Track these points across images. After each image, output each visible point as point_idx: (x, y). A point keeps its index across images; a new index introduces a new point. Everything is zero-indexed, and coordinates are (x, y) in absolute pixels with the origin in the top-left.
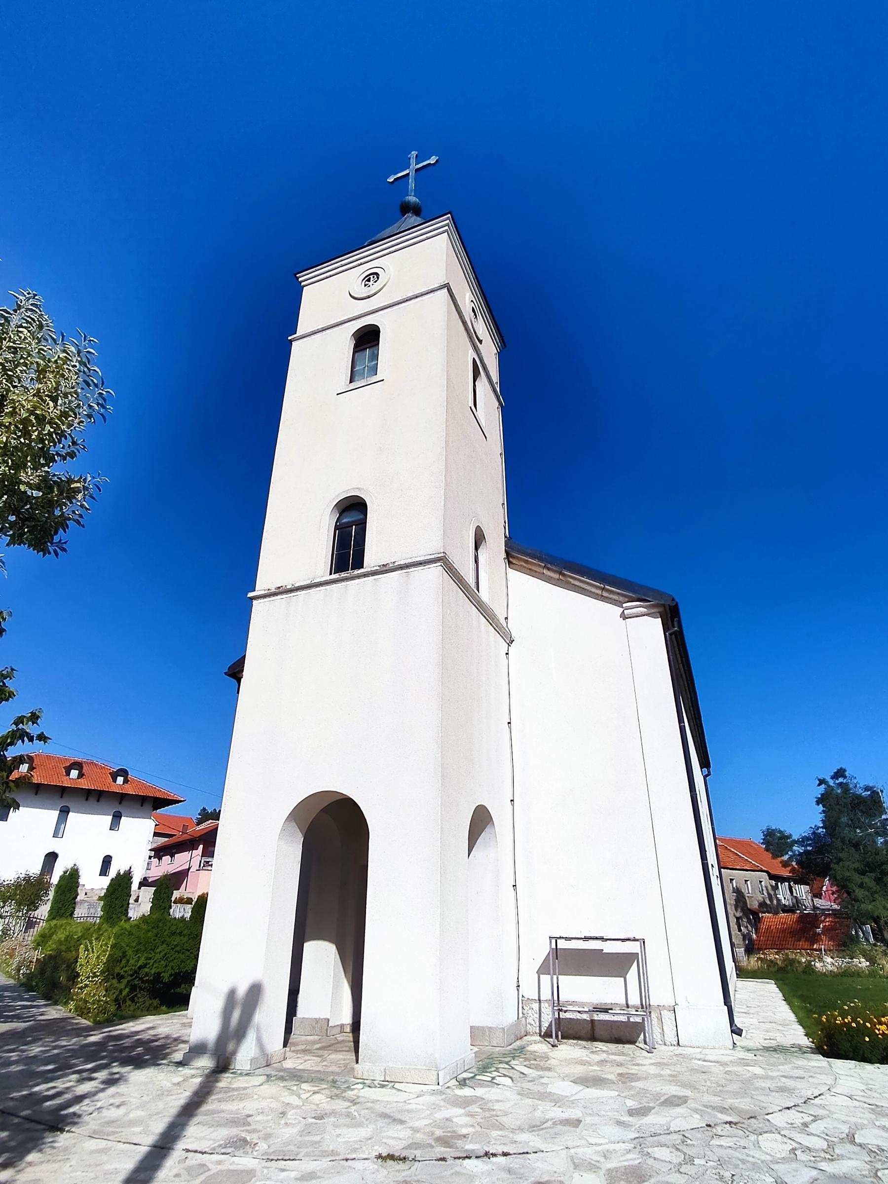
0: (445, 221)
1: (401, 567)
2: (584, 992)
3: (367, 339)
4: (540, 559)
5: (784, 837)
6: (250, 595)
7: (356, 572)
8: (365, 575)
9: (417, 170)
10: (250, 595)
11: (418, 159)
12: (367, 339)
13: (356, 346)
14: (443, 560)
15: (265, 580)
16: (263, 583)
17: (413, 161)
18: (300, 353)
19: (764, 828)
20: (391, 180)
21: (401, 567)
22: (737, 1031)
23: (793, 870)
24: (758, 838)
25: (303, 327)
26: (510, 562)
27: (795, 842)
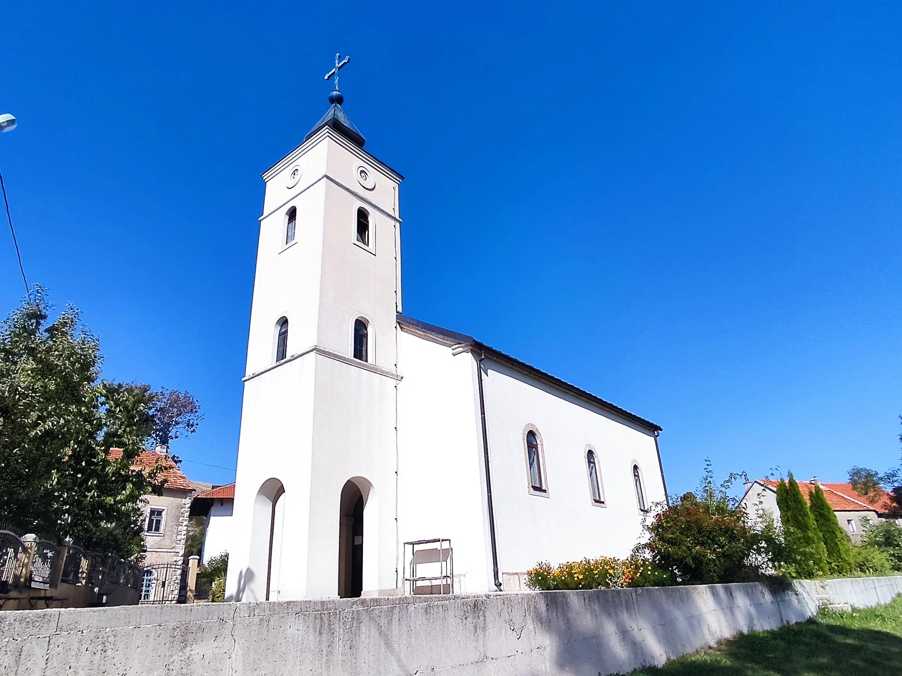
0: (326, 129)
1: (300, 356)
2: (430, 571)
3: (292, 214)
5: (869, 475)
7: (283, 361)
9: (339, 68)
11: (340, 60)
12: (292, 214)
13: (289, 219)
14: (315, 349)
15: (249, 372)
19: (850, 468)
20: (326, 77)
21: (300, 356)
22: (499, 585)
23: (885, 506)
24: (845, 479)
25: (267, 210)
26: (401, 328)
27: (881, 479)
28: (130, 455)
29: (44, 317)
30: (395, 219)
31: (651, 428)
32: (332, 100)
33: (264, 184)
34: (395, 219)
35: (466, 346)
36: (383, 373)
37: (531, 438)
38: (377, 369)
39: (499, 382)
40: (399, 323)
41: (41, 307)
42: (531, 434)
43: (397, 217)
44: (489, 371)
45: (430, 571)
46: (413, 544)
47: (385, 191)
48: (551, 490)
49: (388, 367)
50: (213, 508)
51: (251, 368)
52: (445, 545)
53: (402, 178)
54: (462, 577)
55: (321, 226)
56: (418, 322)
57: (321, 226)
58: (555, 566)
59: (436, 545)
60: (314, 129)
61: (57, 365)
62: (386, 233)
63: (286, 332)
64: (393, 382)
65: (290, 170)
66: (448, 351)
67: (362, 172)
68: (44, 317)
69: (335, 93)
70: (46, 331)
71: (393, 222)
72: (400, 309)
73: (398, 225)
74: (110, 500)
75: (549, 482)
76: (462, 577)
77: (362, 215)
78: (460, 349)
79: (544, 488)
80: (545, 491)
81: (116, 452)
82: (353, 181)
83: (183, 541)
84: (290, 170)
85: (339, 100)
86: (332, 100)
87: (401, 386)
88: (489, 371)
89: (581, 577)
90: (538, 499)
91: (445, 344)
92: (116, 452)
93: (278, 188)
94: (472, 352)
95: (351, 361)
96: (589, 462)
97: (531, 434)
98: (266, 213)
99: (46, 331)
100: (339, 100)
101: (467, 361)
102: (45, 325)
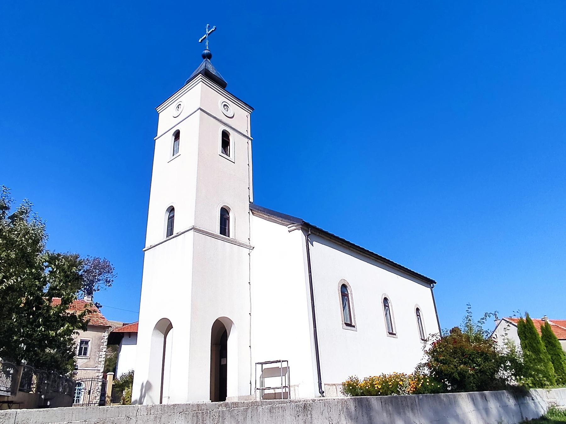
0: (200, 77)
2: (274, 382)
3: (177, 135)
4: (261, 210)
6: (144, 250)
7: (171, 237)
8: (173, 238)
9: (209, 34)
10: (144, 250)
11: (210, 28)
13: (175, 139)
14: (193, 228)
16: (148, 245)
17: (207, 30)
18: (159, 144)
20: (200, 41)
22: (322, 393)
26: (253, 213)
28: (66, 302)
29: (7, 208)
30: (248, 137)
31: (428, 282)
32: (204, 56)
33: (158, 115)
34: (248, 137)
35: (298, 225)
36: (240, 245)
37: (344, 289)
38: (236, 242)
39: (320, 249)
40: (251, 210)
41: (6, 201)
42: (344, 287)
43: (250, 137)
44: (314, 243)
45: (274, 382)
46: (262, 364)
47: (241, 119)
48: (357, 326)
49: (244, 240)
50: (123, 339)
51: (150, 241)
52: (284, 365)
53: (253, 109)
54: (296, 387)
55: (197, 142)
56: (264, 209)
57: (197, 142)
58: (361, 379)
59: (278, 365)
60: (192, 76)
61: (16, 241)
62: (241, 147)
63: (173, 216)
64: (247, 251)
65: (175, 105)
66: (285, 229)
67: (225, 105)
68: (7, 208)
69: (206, 51)
70: (9, 218)
71: (247, 140)
72: (252, 200)
73: (250, 142)
74: (52, 333)
75: (357, 320)
76: (296, 387)
77: (225, 136)
78: (294, 228)
79: (353, 324)
80: (354, 326)
81: (57, 301)
82: (219, 112)
83: (103, 362)
84: (175, 105)
85: (209, 56)
86: (204, 56)
87: (253, 253)
88: (314, 243)
89: (379, 387)
90: (349, 332)
91: (283, 224)
92: (57, 301)
93: (167, 117)
94: (303, 229)
95: (218, 236)
96: (385, 306)
97: (344, 287)
98: (159, 135)
99: (9, 218)
100: (209, 56)
101: (299, 235)
102: (9, 213)
